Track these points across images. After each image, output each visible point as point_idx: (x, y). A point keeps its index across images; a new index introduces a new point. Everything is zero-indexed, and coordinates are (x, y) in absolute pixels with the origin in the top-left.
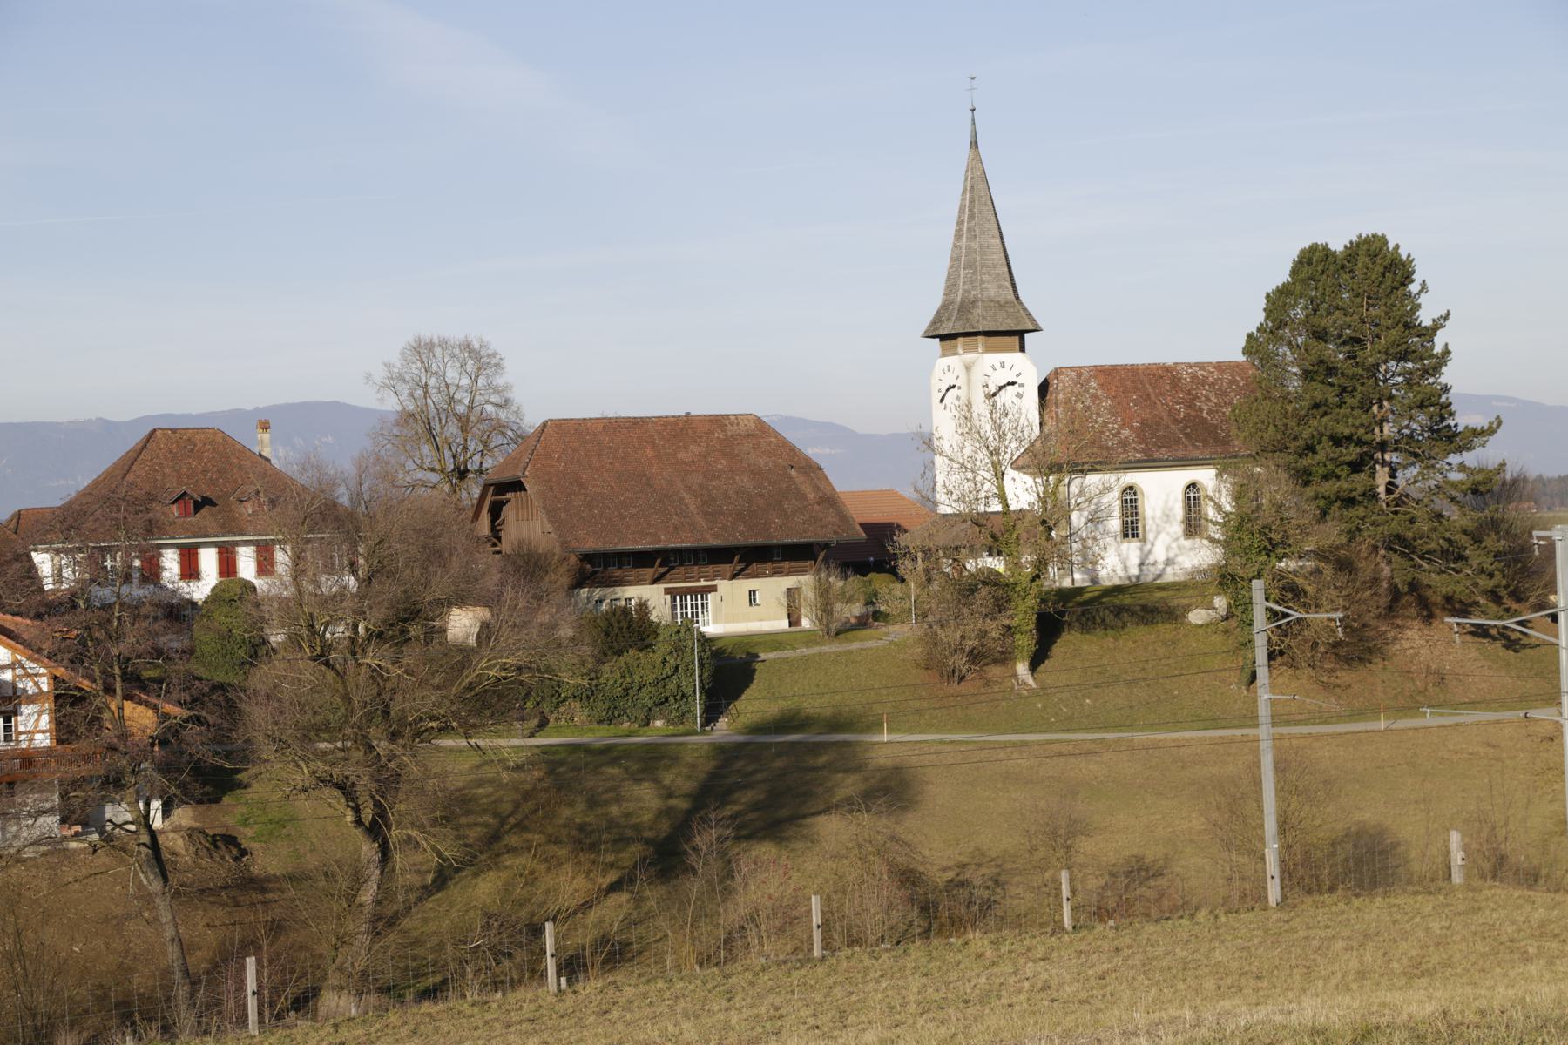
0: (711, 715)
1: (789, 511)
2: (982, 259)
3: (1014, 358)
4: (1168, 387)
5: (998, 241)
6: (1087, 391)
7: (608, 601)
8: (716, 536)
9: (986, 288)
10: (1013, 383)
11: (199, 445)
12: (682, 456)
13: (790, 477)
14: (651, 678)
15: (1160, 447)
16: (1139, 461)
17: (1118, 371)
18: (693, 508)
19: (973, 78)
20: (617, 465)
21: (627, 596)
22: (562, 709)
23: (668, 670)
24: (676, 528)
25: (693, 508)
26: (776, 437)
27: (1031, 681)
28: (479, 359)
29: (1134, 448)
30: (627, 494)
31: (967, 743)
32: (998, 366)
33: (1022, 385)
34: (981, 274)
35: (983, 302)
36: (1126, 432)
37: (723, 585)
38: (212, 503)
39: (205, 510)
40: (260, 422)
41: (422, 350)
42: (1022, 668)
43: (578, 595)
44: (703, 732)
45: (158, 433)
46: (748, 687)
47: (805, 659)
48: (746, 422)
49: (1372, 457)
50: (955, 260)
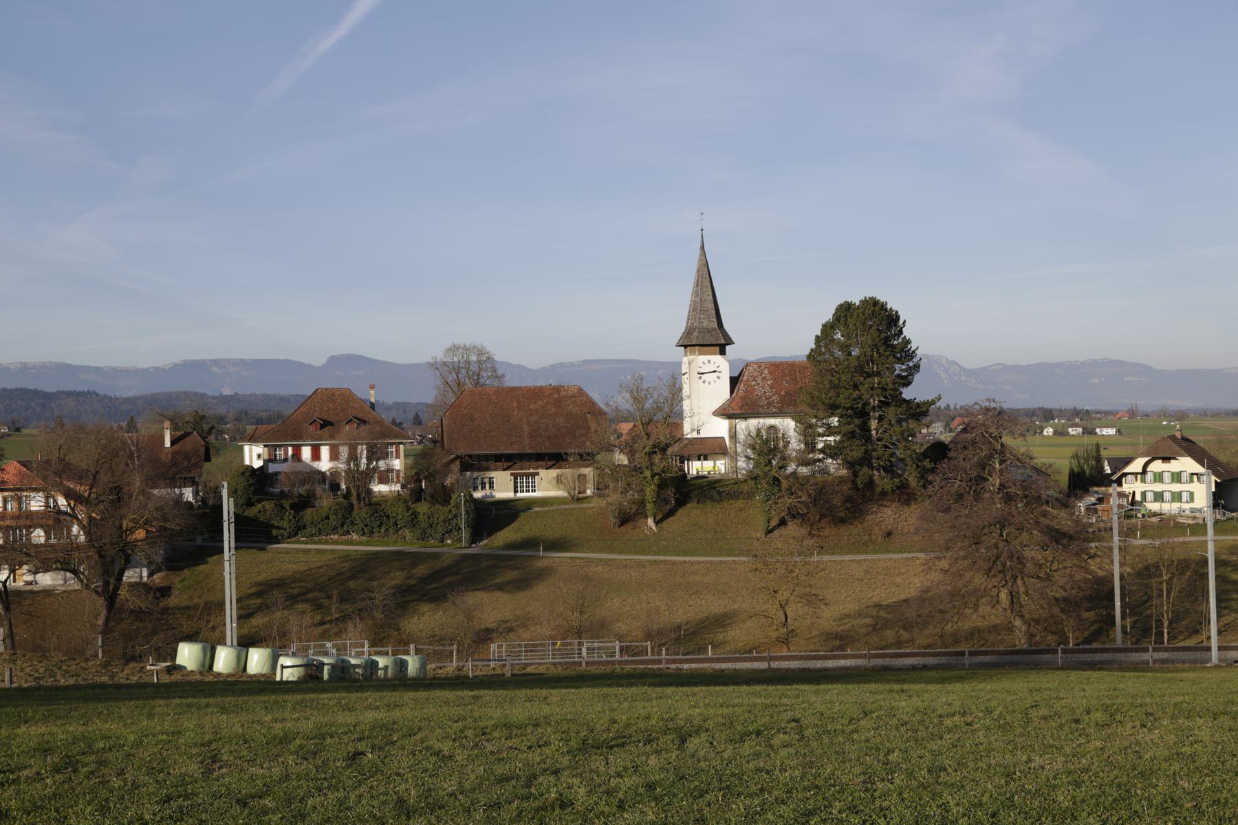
0: (476, 537)
3: (717, 360)
5: (711, 297)
6: (761, 375)
8: (531, 448)
10: (715, 371)
11: (337, 396)
12: (532, 406)
14: (441, 519)
16: (774, 413)
18: (526, 434)
21: (491, 476)
22: (400, 533)
23: (450, 517)
24: (512, 443)
25: (526, 434)
27: (654, 528)
28: (481, 352)
31: (583, 558)
32: (706, 362)
33: (720, 372)
36: (774, 398)
37: (543, 472)
38: (331, 424)
39: (326, 429)
41: (454, 349)
42: (650, 522)
43: (465, 474)
44: (470, 547)
45: (319, 391)
46: (510, 524)
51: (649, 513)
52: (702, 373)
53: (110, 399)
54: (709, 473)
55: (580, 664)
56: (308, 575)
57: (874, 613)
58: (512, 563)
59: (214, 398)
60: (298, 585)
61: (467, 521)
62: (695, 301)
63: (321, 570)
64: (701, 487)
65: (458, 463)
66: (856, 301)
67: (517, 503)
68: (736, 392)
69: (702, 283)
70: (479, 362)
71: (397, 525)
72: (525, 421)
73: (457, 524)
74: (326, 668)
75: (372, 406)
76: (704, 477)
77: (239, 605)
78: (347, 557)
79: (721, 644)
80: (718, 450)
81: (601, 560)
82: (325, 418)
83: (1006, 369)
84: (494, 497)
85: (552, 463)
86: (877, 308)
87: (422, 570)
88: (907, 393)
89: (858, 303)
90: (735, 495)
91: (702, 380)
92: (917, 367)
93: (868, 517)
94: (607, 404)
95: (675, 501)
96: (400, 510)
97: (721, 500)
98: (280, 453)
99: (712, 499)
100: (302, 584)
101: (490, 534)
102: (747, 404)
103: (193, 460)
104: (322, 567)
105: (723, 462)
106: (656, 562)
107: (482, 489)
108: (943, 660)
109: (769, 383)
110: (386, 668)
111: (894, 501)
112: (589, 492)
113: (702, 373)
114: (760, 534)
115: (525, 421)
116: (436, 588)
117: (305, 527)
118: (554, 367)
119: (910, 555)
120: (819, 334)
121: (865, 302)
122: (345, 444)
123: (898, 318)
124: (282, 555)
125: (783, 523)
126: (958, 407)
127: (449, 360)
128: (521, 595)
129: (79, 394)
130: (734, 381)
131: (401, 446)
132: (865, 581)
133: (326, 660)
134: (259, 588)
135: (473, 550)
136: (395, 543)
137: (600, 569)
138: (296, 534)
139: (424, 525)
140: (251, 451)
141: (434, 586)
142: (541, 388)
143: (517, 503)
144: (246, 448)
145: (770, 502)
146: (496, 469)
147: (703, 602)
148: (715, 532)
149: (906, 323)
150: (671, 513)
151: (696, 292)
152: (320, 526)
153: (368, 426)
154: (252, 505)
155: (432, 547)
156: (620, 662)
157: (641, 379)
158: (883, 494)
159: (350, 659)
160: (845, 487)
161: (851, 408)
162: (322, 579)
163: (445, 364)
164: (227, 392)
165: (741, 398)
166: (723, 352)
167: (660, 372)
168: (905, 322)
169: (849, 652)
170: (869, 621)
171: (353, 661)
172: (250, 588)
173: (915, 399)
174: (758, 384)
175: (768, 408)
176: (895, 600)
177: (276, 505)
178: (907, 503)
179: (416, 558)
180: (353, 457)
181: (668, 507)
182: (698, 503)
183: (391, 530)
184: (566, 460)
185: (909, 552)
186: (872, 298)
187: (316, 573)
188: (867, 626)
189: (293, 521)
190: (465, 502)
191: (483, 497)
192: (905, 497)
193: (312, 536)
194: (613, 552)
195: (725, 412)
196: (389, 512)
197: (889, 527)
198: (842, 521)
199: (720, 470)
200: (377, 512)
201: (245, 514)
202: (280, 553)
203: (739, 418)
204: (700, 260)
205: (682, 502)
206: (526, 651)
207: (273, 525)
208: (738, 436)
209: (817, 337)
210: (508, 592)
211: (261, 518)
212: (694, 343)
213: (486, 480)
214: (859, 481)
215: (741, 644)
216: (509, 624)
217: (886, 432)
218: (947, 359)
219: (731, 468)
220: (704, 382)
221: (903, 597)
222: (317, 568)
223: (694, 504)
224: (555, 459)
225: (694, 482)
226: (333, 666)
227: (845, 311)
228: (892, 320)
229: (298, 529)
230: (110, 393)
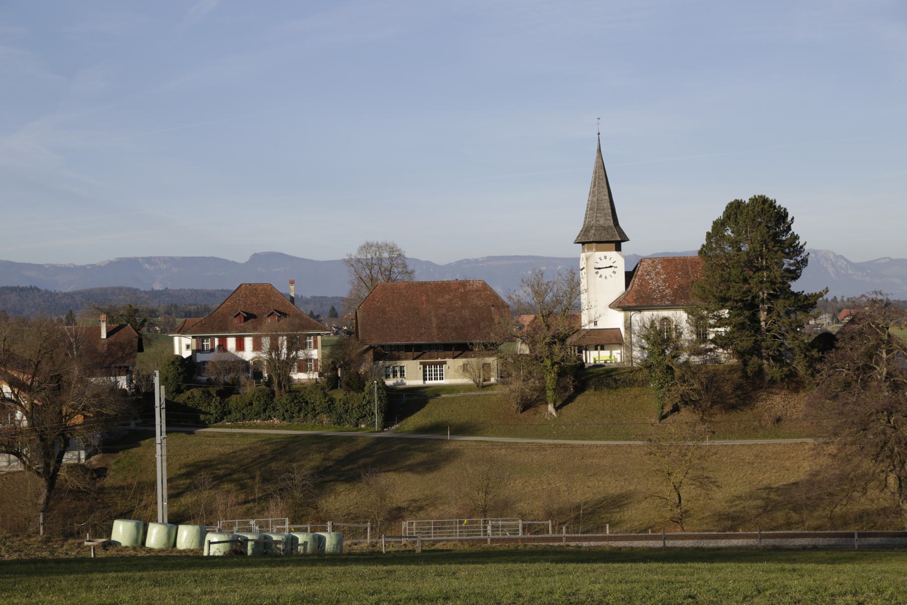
0: (388, 421)
1: (482, 327)
2: (598, 205)
3: (614, 255)
4: (700, 268)
5: (607, 197)
6: (654, 270)
7: (391, 367)
9: (599, 221)
10: (611, 267)
11: (259, 291)
12: (440, 300)
13: (490, 311)
14: (356, 405)
15: (682, 299)
16: (667, 306)
17: (676, 260)
18: (434, 325)
19: (599, 119)
20: (406, 304)
21: (402, 365)
22: (318, 418)
23: (364, 403)
24: (421, 334)
26: (491, 291)
27: (554, 414)
28: (392, 250)
29: (668, 300)
30: (405, 318)
31: (485, 442)
32: (603, 258)
33: (616, 267)
34: (597, 213)
35: (596, 227)
36: (667, 291)
37: (450, 361)
38: (254, 317)
39: (249, 321)
40: (290, 281)
41: (367, 247)
42: (551, 408)
43: (378, 363)
44: (382, 431)
45: (243, 286)
46: (419, 410)
47: (453, 399)
48: (478, 284)
49: (758, 307)
50: (588, 204)
51: (549, 400)
52: (599, 268)
53: (51, 294)
54: (606, 362)
55: (485, 541)
56: (233, 457)
57: (764, 495)
58: (422, 446)
59: (146, 292)
60: (223, 466)
61: (380, 408)
62: (592, 201)
63: (245, 452)
64: (598, 375)
65: (371, 352)
66: (746, 199)
67: (426, 390)
68: (630, 286)
69: (599, 183)
70: (391, 259)
71: (315, 410)
72: (433, 313)
73: (370, 409)
74: (250, 544)
75: (292, 300)
76: (601, 366)
77: (169, 485)
78: (269, 440)
79: (617, 523)
80: (614, 341)
81: (505, 443)
82: (249, 311)
83: (892, 263)
84: (405, 384)
85: (458, 353)
86: (766, 206)
87: (339, 453)
88: (795, 286)
89: (747, 201)
90: (631, 383)
91: (599, 275)
92: (805, 262)
93: (758, 404)
94: (510, 298)
95: (574, 388)
96: (318, 397)
97: (617, 388)
98: (207, 344)
99: (608, 386)
100: (226, 465)
101: (401, 419)
102: (642, 297)
103: (127, 351)
104: (245, 449)
105: (619, 351)
106: (556, 445)
107: (394, 377)
108: (833, 541)
109: (662, 277)
110: (305, 544)
111: (783, 388)
112: (493, 380)
113: (599, 268)
114: (655, 420)
115: (433, 313)
116: (351, 469)
117: (230, 413)
118: (460, 263)
119: (799, 441)
120: (710, 231)
121: (754, 200)
122: (267, 335)
123: (786, 215)
124: (210, 439)
125: (676, 409)
126: (845, 299)
127: (363, 257)
128: (430, 476)
129: (23, 289)
130: (629, 276)
131: (319, 338)
132: (755, 465)
133: (250, 537)
134: (188, 469)
135: (386, 434)
136: (313, 428)
137: (503, 451)
138: (222, 419)
139: (340, 410)
140: (180, 342)
141: (349, 467)
142: (448, 284)
143: (426, 390)
144: (176, 339)
145: (664, 389)
146: (406, 359)
147: (601, 483)
148: (612, 417)
149: (794, 220)
150: (570, 399)
151: (594, 192)
152: (244, 411)
153: (288, 319)
154: (182, 392)
155: (347, 431)
156: (523, 540)
157: (542, 274)
158: (773, 382)
159: (272, 536)
160: (735, 375)
161: (741, 300)
162: (246, 460)
163: (359, 261)
164: (158, 287)
165: (636, 291)
166: (618, 249)
167: (559, 267)
168: (793, 218)
169: (741, 532)
170: (759, 502)
171: (275, 538)
172: (179, 469)
173: (803, 292)
174: (652, 279)
175: (662, 300)
176: (785, 483)
177: (203, 392)
178: (796, 390)
179: (333, 442)
180: (275, 347)
181: (567, 394)
182: (595, 390)
183: (309, 415)
184: (471, 350)
185: (798, 437)
186: (761, 196)
187: (240, 455)
188: (759, 507)
189: (219, 407)
190: (378, 389)
191: (394, 384)
192: (794, 385)
193: (237, 420)
194: (515, 436)
195: (620, 305)
196: (308, 399)
197: (779, 414)
198: (733, 407)
199: (616, 359)
200: (296, 398)
201: (175, 400)
202: (207, 436)
203: (634, 310)
204: (597, 162)
205: (580, 389)
206: (435, 529)
207: (200, 410)
208: (633, 327)
209: (708, 234)
210: (418, 473)
211: (190, 404)
212: (592, 240)
213: (398, 369)
214: (749, 370)
215: (637, 524)
216: (419, 504)
217: (775, 323)
218: (834, 254)
219: (627, 357)
220: (601, 276)
221: (792, 480)
222: (241, 450)
223: (592, 391)
224: (461, 349)
225: (591, 370)
226: (256, 542)
227: (735, 209)
228: (781, 217)
229: (224, 414)
230: (51, 289)
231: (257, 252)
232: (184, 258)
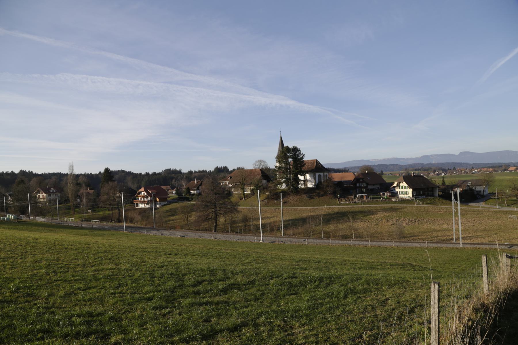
129: (394, 165)
164: (434, 162)
231: (462, 151)
232: (441, 155)
